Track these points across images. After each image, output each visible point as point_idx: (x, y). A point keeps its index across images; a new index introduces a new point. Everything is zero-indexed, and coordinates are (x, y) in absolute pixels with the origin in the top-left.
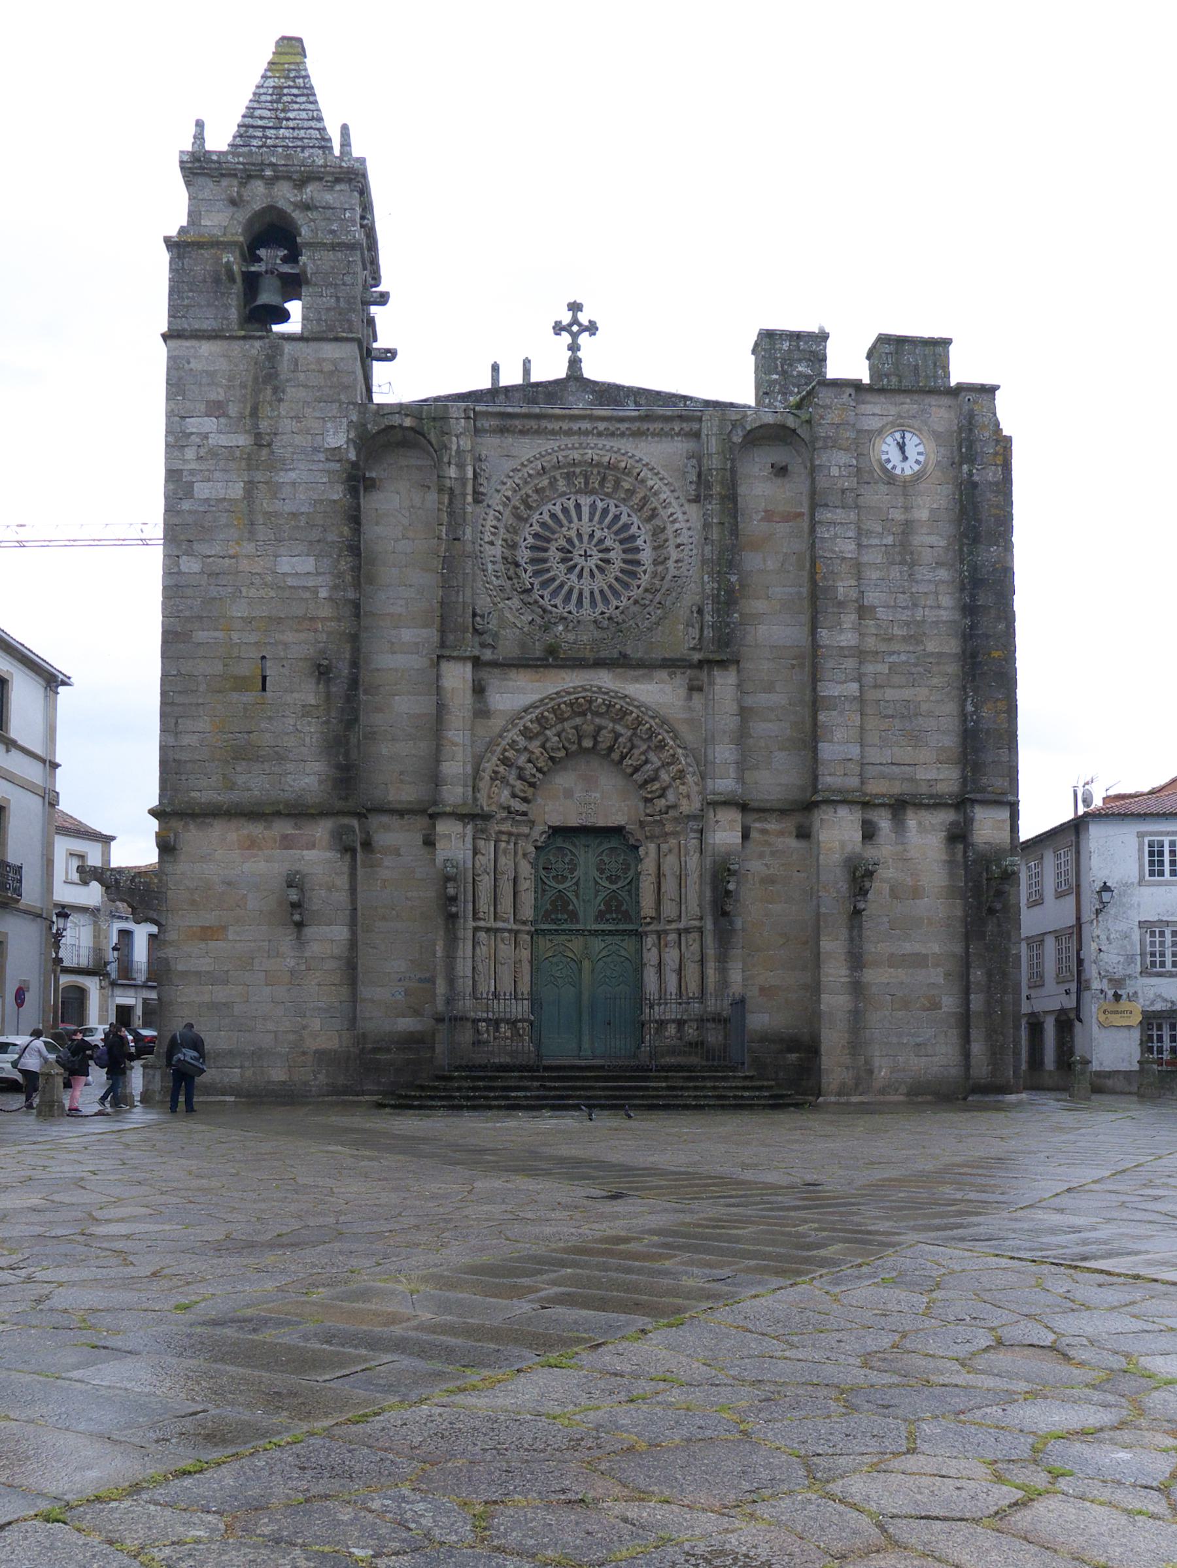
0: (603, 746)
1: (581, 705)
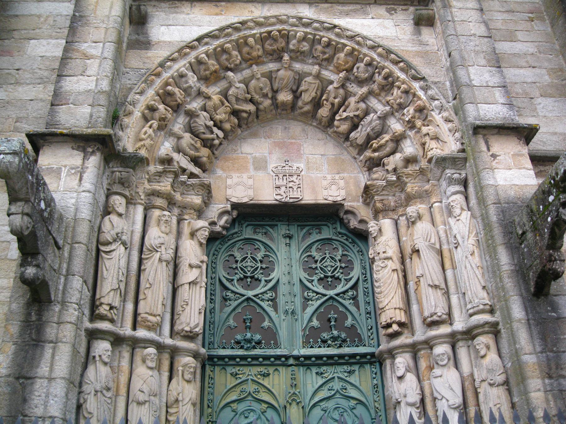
0: (306, 97)
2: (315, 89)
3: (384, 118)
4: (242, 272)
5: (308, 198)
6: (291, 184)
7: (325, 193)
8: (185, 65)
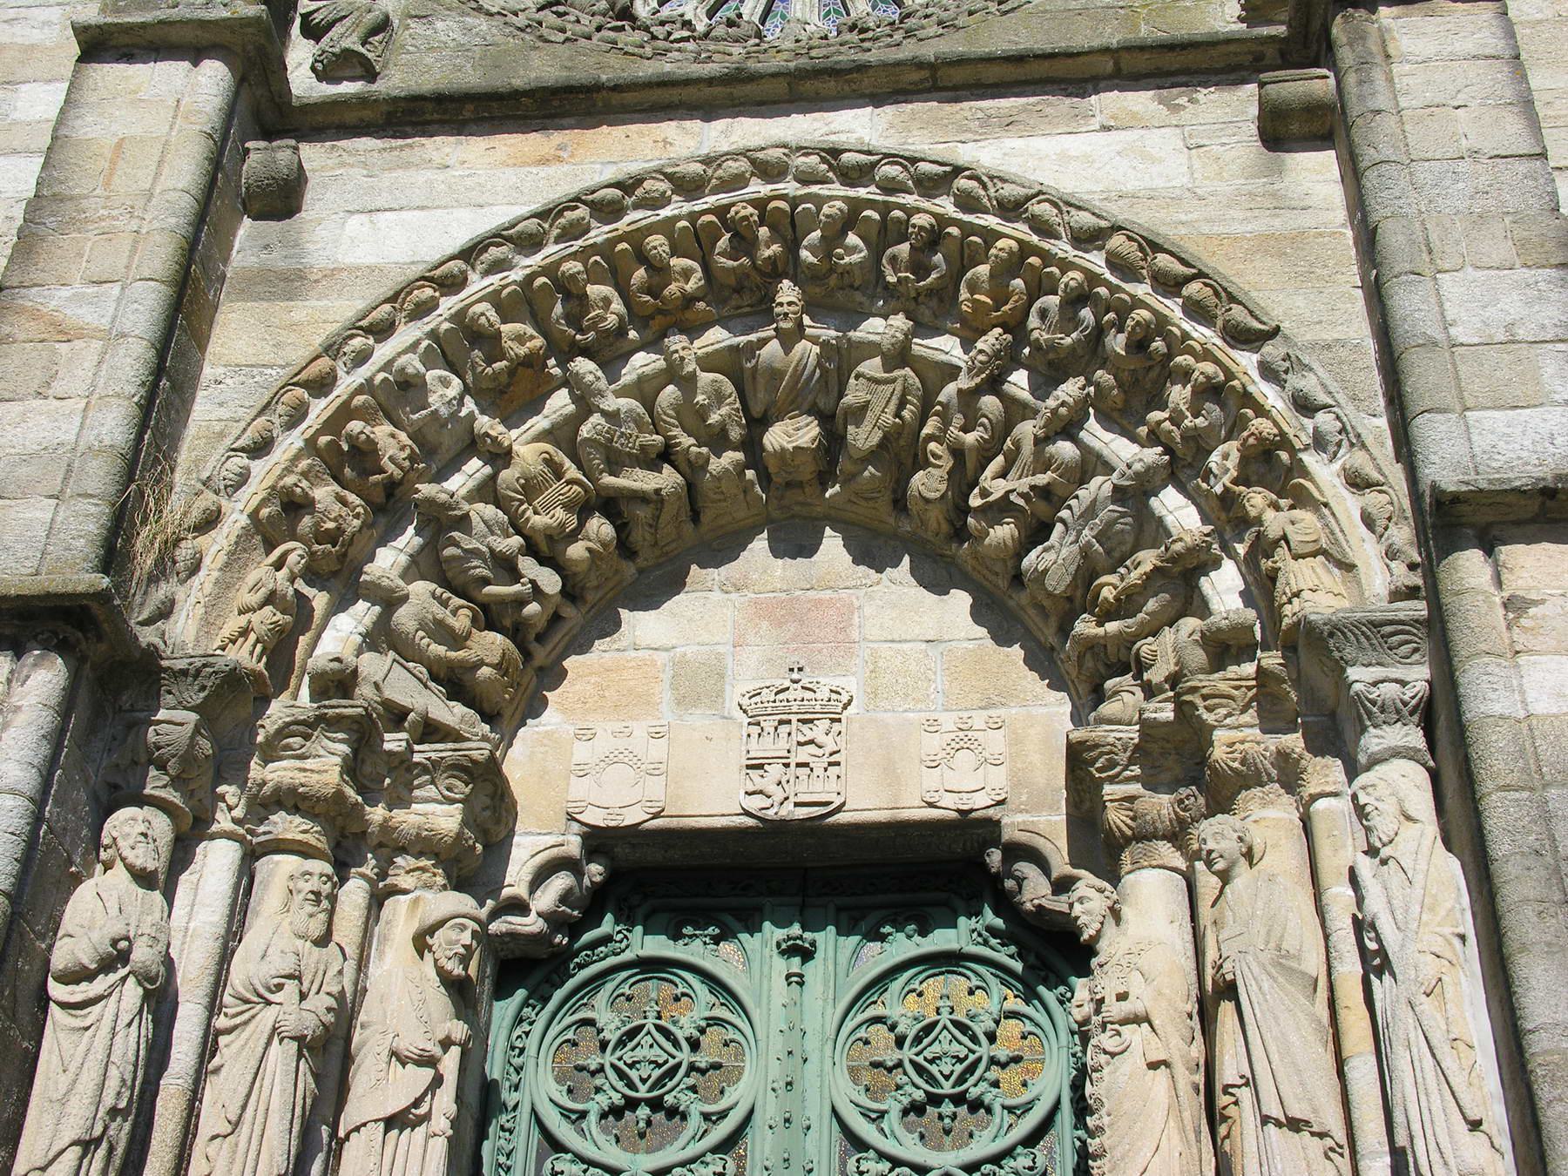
0: (863, 437)
2: (895, 401)
3: (1135, 494)
4: (620, 1085)
5: (865, 799)
6: (803, 754)
7: (932, 780)
8: (413, 347)
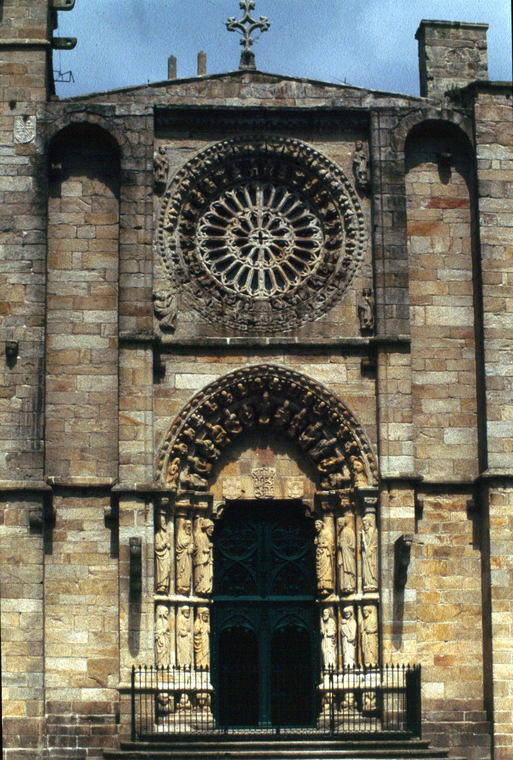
1: (257, 384)
